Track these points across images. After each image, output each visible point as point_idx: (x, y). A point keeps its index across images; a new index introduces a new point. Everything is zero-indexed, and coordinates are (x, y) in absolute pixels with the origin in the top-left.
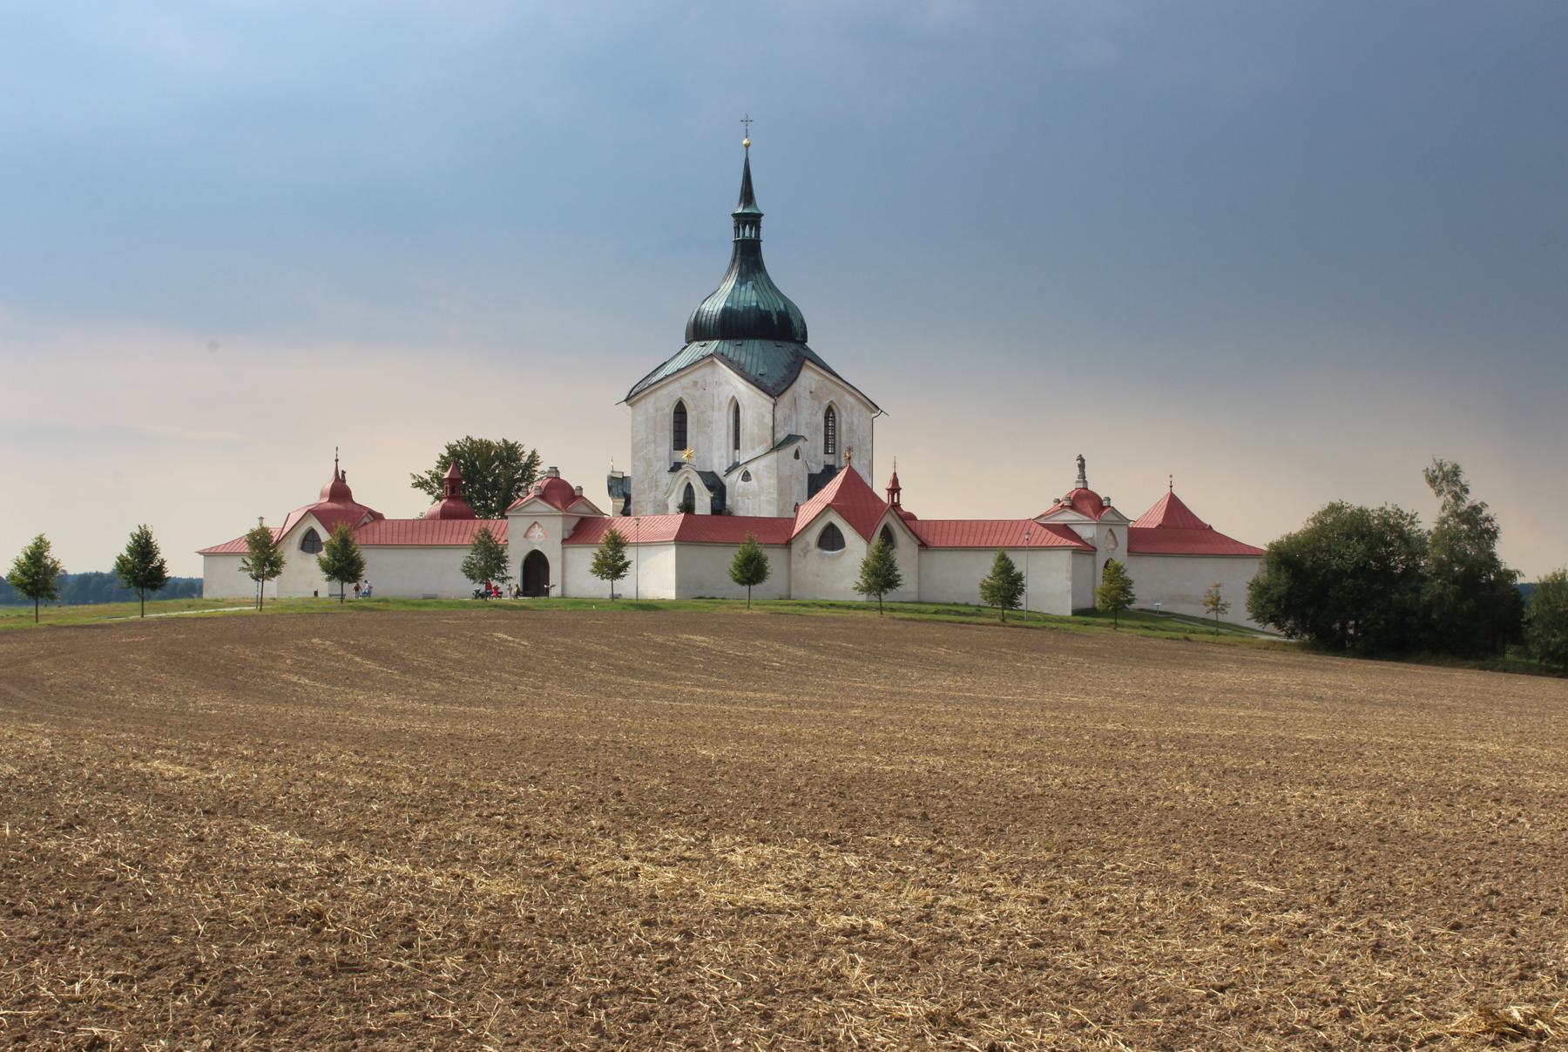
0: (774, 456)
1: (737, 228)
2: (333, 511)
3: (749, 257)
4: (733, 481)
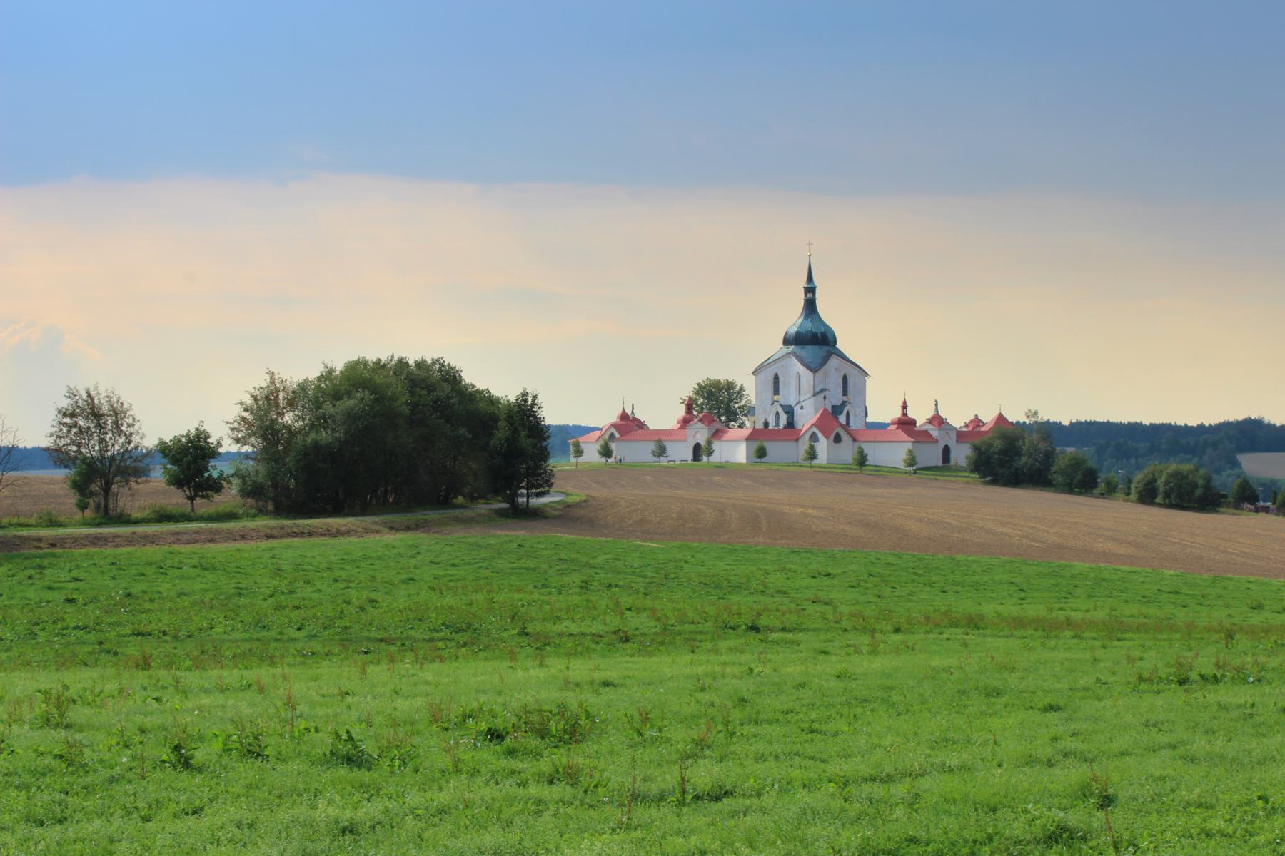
0: (813, 399)
1: (806, 296)
2: (622, 425)
3: (810, 307)
4: (797, 409)
